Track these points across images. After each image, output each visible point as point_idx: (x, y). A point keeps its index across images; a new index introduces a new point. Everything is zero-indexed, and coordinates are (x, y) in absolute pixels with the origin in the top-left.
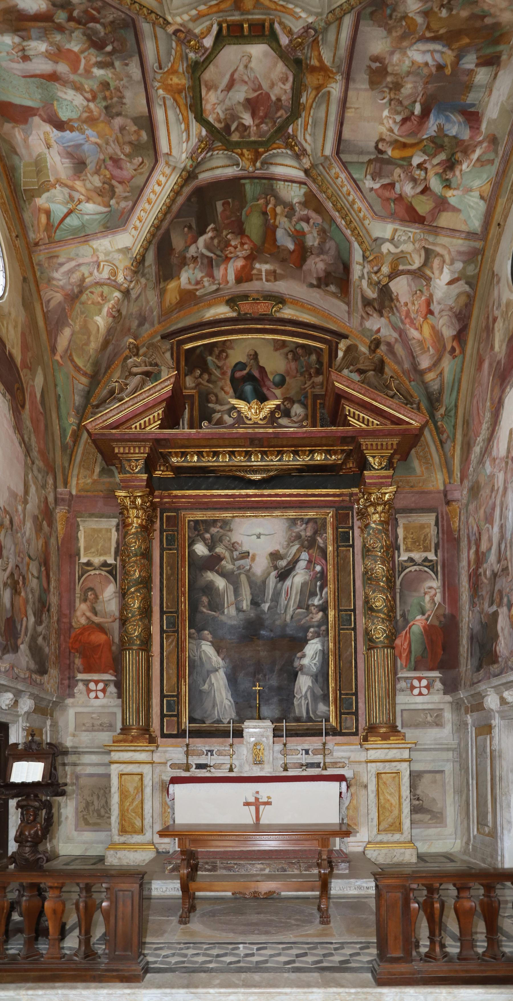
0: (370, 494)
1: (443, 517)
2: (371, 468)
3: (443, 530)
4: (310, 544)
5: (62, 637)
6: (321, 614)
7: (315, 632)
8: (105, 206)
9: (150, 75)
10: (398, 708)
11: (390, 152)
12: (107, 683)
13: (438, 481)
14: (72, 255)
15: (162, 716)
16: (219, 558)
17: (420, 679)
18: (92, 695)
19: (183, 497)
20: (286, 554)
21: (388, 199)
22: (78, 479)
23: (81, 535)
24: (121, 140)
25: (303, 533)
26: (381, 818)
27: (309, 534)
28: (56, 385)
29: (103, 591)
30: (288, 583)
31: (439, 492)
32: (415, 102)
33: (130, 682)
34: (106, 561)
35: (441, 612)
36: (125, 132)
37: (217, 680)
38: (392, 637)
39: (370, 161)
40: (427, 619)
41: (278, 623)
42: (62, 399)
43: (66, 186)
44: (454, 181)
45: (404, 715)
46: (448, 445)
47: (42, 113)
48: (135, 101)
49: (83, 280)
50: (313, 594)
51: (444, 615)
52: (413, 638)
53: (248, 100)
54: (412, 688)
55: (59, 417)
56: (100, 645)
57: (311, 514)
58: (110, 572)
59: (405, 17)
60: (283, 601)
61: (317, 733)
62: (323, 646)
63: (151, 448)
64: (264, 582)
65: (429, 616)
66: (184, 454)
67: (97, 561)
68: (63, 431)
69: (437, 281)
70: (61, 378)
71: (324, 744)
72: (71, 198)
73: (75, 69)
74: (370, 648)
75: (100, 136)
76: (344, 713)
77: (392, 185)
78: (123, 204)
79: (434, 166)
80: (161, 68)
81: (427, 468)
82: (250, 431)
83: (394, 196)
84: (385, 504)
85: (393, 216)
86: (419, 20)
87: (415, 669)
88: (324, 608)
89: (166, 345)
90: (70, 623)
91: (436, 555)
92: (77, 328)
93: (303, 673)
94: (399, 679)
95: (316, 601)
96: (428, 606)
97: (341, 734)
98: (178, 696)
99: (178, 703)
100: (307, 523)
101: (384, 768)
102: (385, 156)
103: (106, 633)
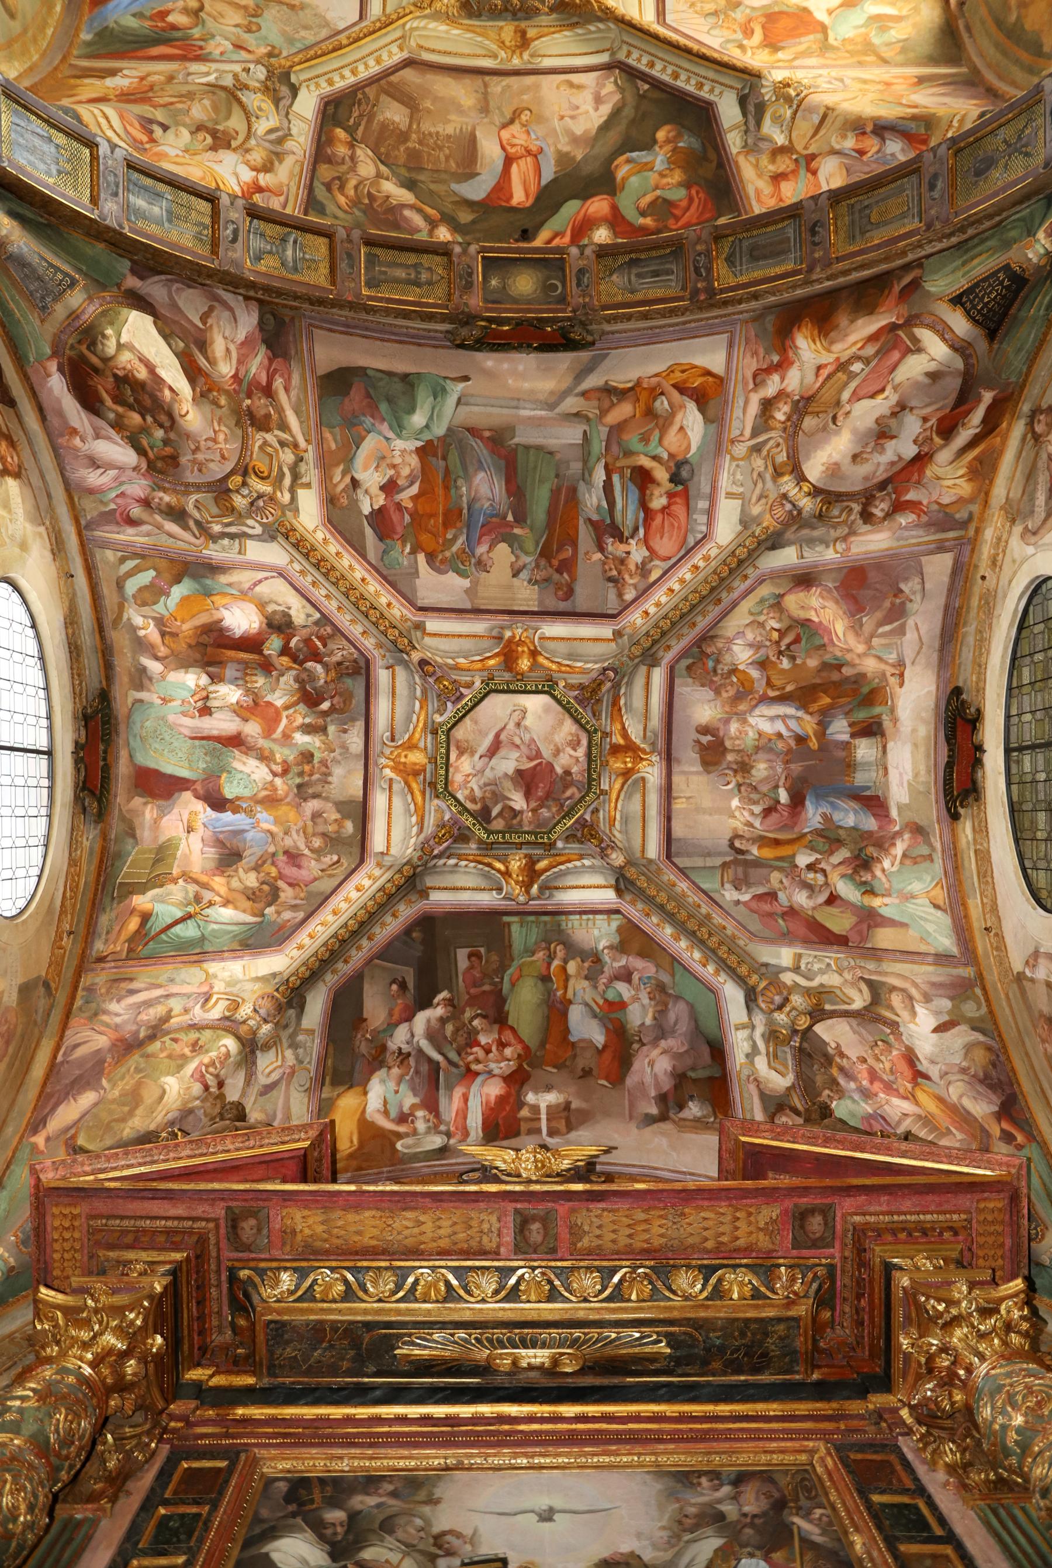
8: (255, 915)
9: (376, 747)
11: (755, 851)
21: (771, 915)
24: (310, 830)
32: (777, 787)
36: (319, 820)
39: (725, 865)
43: (196, 882)
44: (876, 884)
47: (198, 787)
48: (346, 780)
53: (519, 772)
59: (734, 671)
72: (198, 899)
73: (268, 733)
75: (276, 822)
77: (772, 896)
78: (287, 915)
79: (835, 866)
80: (393, 740)
83: (779, 910)
85: (786, 938)
86: (755, 673)
102: (749, 857)
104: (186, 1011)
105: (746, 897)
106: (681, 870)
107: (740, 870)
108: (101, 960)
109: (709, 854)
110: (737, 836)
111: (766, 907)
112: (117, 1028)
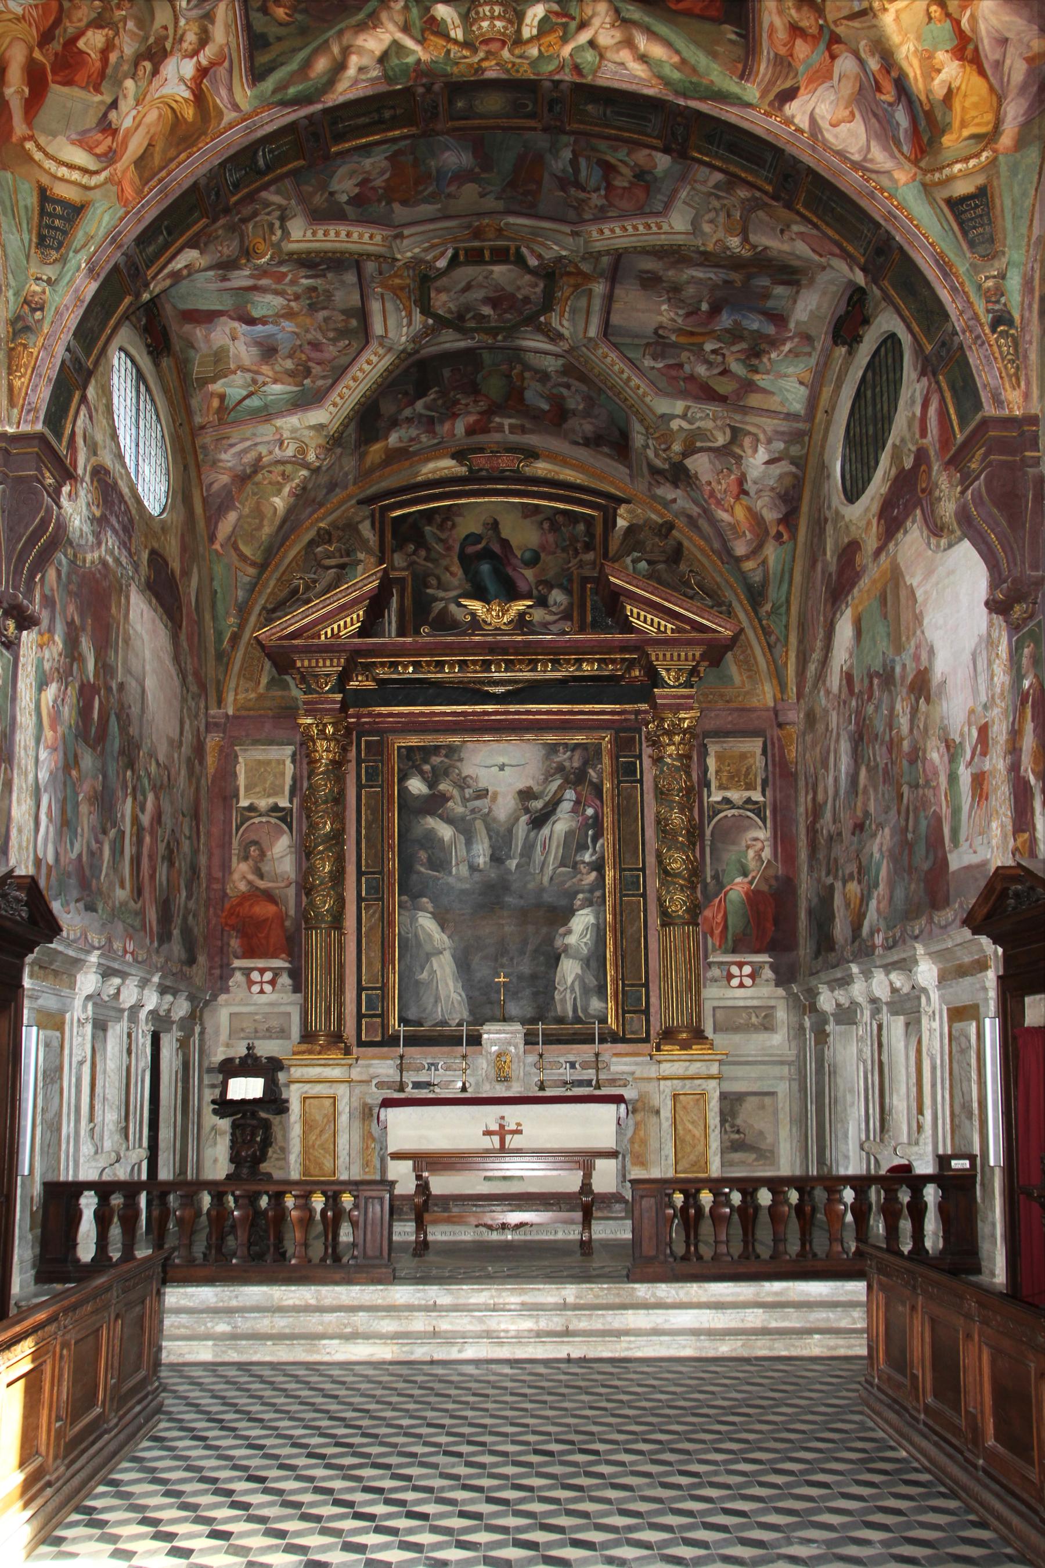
0: (663, 720)
1: (773, 744)
2: (664, 684)
3: (773, 761)
4: (577, 778)
5: (211, 910)
6: (594, 874)
7: (585, 899)
10: (708, 1007)
12: (277, 972)
13: (766, 694)
14: (248, 434)
15: (360, 1016)
16: (444, 798)
17: (740, 965)
18: (256, 988)
19: (391, 715)
20: (542, 792)
21: (675, 378)
22: (236, 694)
23: (241, 770)
25: (567, 764)
26: (679, 1155)
27: (576, 765)
28: (212, 579)
29: (272, 845)
30: (546, 831)
31: (767, 710)
33: (316, 974)
34: (276, 804)
35: (771, 872)
37: (442, 967)
38: (694, 911)
39: (648, 345)
40: (751, 883)
41: (531, 886)
42: (219, 595)
45: (718, 1015)
46: (779, 650)
49: (260, 458)
50: (582, 847)
51: (776, 878)
52: (729, 908)
54: (730, 976)
55: (214, 618)
56: (267, 920)
57: (580, 738)
58: (283, 819)
60: (538, 855)
61: (587, 1039)
62: (597, 918)
63: (347, 660)
64: (510, 831)
65: (754, 878)
66: (394, 665)
67: (263, 804)
68: (219, 635)
69: (751, 460)
70: (219, 569)
71: (597, 1055)
72: (254, 381)
74: (664, 925)
76: (629, 1012)
77: (680, 366)
81: (750, 677)
82: (490, 639)
84: (685, 732)
85: (683, 394)
87: (734, 951)
88: (599, 867)
89: (366, 511)
90: (224, 890)
91: (764, 795)
92: (246, 511)
93: (568, 956)
94: (710, 965)
95: (587, 857)
96: (752, 864)
97: (624, 1040)
98: (384, 988)
99: (384, 998)
100: (573, 750)
101: (683, 1087)
103: (276, 903)
104: (271, 453)
105: (660, 365)
106: (614, 345)
107: (659, 348)
108: (203, 427)
109: (637, 336)
110: (661, 327)
111: (674, 373)
112: (230, 469)
